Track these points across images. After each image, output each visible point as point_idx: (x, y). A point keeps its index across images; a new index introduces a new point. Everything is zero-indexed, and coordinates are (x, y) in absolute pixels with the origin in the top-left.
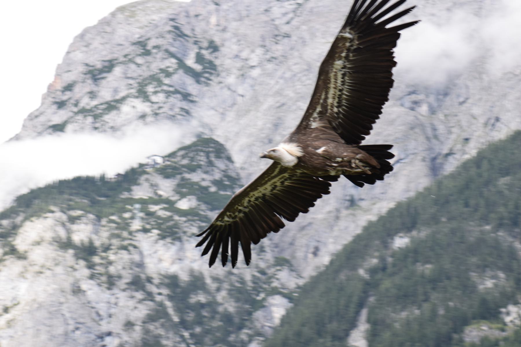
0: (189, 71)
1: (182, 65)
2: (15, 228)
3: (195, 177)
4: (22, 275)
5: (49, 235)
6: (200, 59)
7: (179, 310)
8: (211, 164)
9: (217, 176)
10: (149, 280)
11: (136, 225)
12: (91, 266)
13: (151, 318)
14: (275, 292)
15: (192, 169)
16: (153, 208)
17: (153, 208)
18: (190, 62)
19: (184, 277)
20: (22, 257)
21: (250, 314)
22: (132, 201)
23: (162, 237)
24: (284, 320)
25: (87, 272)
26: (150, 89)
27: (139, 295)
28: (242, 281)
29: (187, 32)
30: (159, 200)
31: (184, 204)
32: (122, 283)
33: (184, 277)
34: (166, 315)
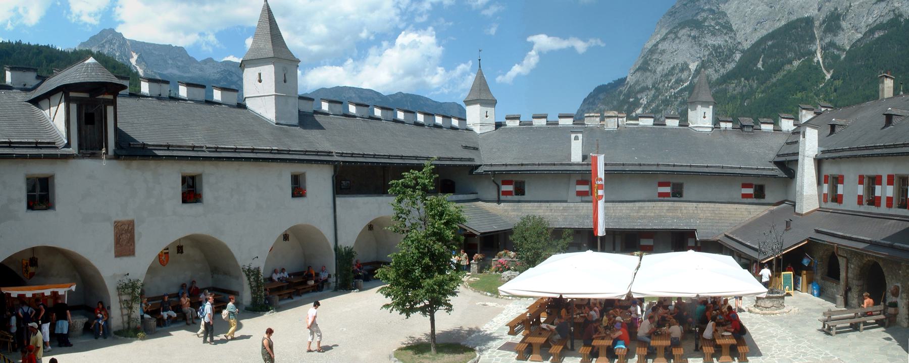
2: (678, 32)
3: (720, 21)
4: (680, 43)
5: (685, 34)
7: (715, 53)
8: (723, 18)
9: (725, 21)
11: (706, 32)
12: (695, 41)
13: (709, 55)
14: (738, 50)
15: (719, 19)
16: (710, 28)
17: (710, 28)
19: (717, 45)
20: (679, 38)
21: (732, 55)
23: (712, 35)
24: (741, 58)
25: (694, 43)
27: (706, 49)
30: (711, 26)
31: (717, 28)
32: (703, 46)
33: (717, 45)
34: (712, 54)
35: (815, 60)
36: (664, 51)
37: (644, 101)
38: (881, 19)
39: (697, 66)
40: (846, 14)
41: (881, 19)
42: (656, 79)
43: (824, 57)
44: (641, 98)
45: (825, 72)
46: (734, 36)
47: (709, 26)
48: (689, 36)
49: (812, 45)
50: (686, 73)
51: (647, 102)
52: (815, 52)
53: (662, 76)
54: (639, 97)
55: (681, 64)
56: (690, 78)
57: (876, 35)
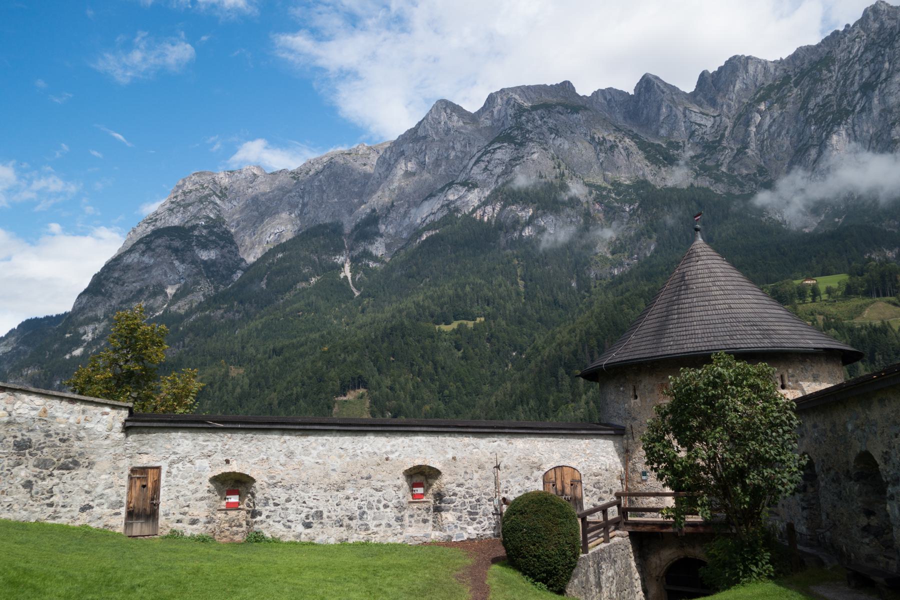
0: (217, 196)
1: (215, 193)
2: (151, 242)
3: (215, 230)
6: (221, 192)
10: (197, 262)
11: (194, 244)
14: (239, 269)
18: (218, 193)
20: (153, 250)
22: (193, 236)
26: (203, 200)
28: (229, 264)
29: (218, 182)
30: (202, 236)
35: (342, 275)
36: (128, 267)
37: (89, 337)
38: (432, 217)
39: (178, 290)
40: (386, 215)
41: (432, 217)
42: (111, 306)
43: (354, 271)
44: (85, 333)
45: (354, 290)
46: (234, 250)
47: (199, 236)
48: (169, 247)
49: (338, 257)
50: (160, 299)
51: (93, 339)
52: (343, 266)
53: (122, 303)
54: (81, 331)
55: (154, 286)
56: (165, 306)
57: (424, 237)
